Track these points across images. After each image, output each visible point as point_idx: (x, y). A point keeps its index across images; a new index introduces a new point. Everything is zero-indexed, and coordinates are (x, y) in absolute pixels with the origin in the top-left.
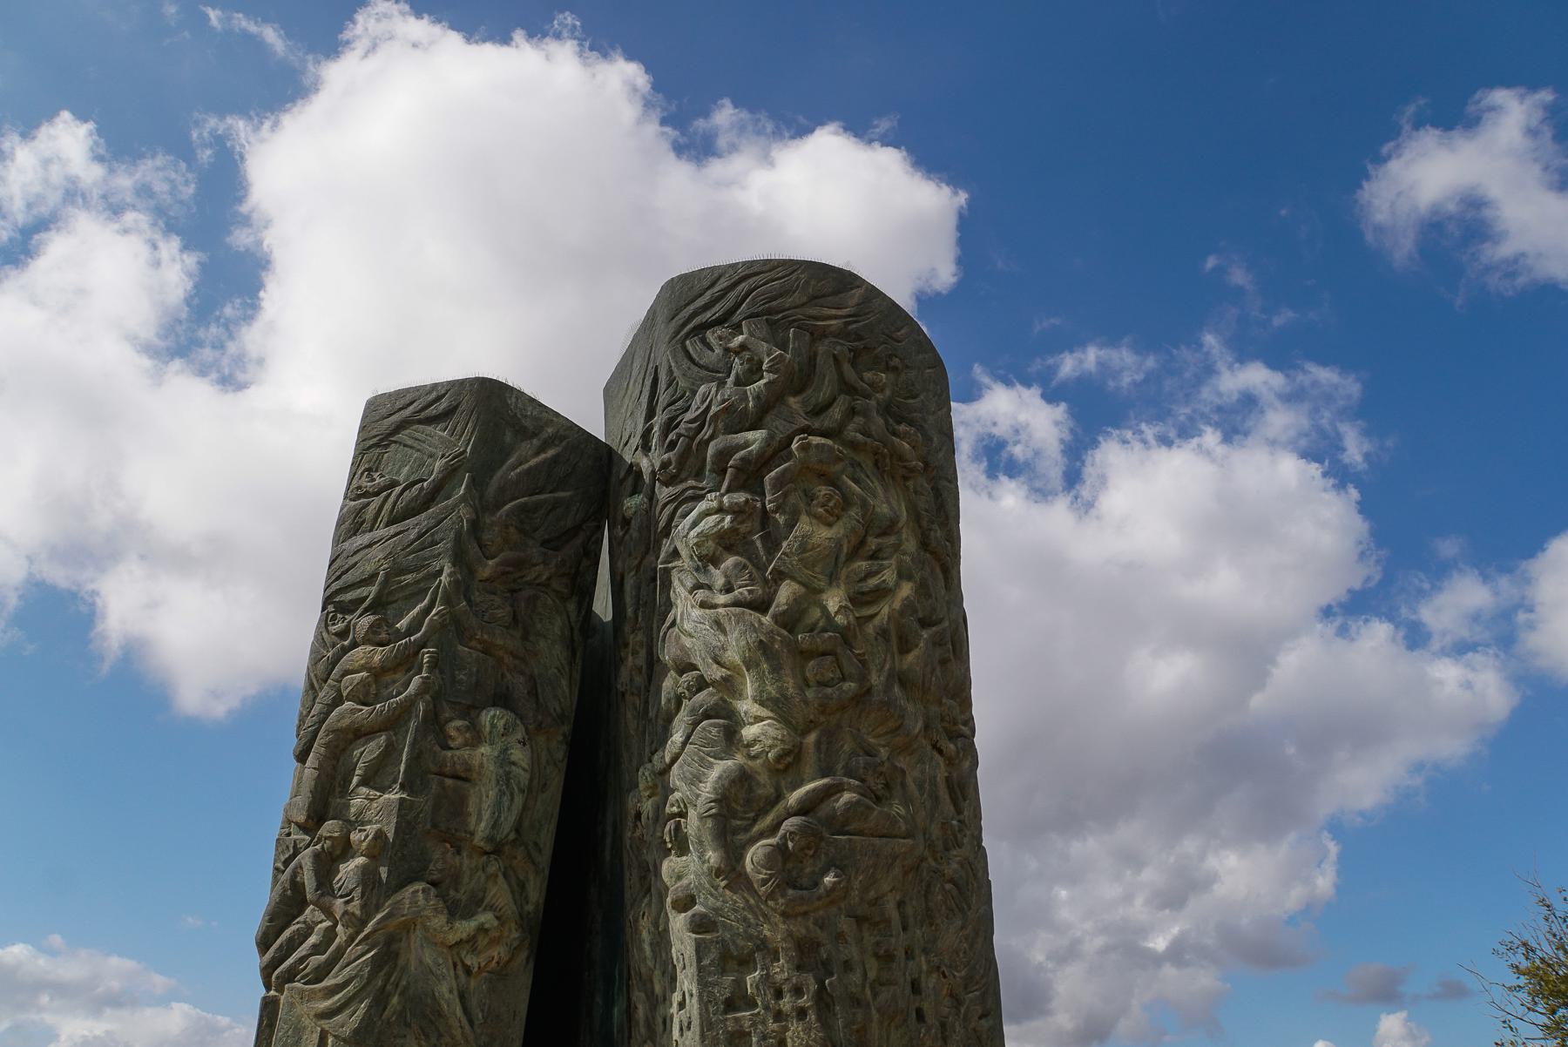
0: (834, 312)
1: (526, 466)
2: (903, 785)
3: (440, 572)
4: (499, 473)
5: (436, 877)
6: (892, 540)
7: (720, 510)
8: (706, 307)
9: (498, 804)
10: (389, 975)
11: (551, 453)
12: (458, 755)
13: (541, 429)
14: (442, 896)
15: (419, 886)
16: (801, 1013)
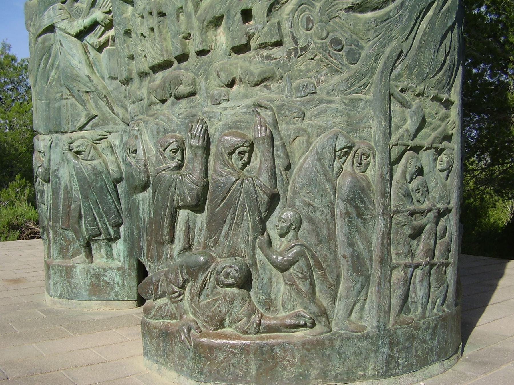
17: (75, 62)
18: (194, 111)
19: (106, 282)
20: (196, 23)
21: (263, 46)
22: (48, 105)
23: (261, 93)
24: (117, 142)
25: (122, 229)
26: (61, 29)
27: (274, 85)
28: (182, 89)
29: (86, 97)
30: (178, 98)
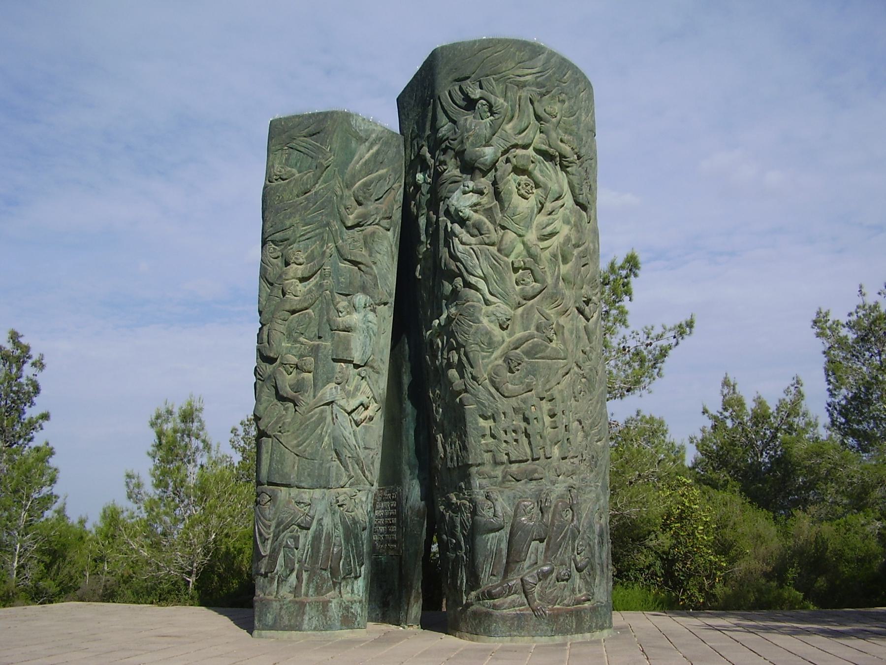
0: (530, 71)
1: (363, 160)
2: (563, 333)
4: (351, 166)
5: (339, 380)
6: (560, 202)
9: (364, 345)
10: (323, 428)
11: (375, 149)
12: (344, 319)
13: (369, 136)
14: (343, 389)
15: (333, 385)
17: (346, 433)
18: (541, 488)
19: (352, 613)
20: (549, 443)
21: (572, 458)
22: (321, 464)
23: (570, 481)
24: (364, 499)
25: (363, 568)
26: (339, 406)
27: (574, 477)
28: (536, 475)
29: (349, 461)
30: (531, 480)
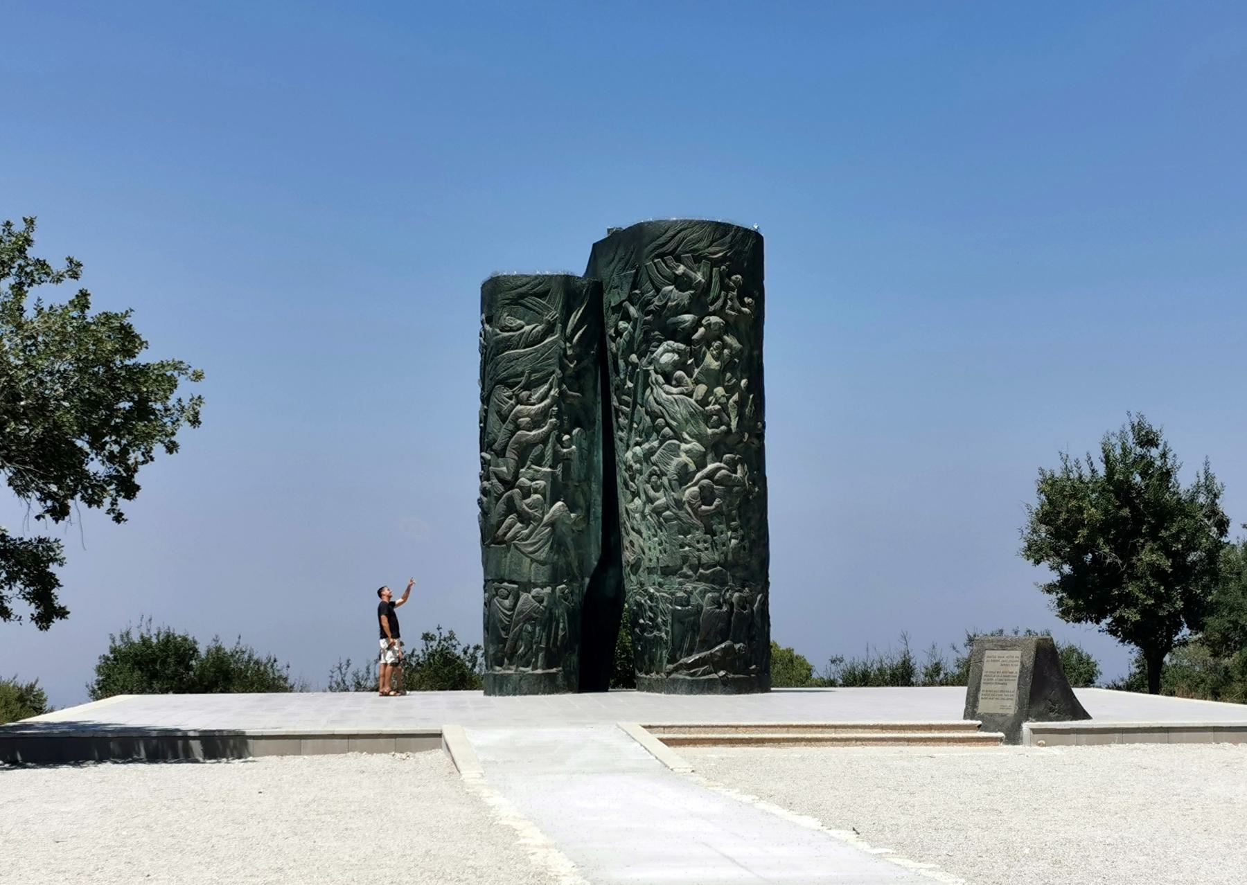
3: (553, 372)
7: (673, 351)
8: (663, 245)
16: (707, 549)
